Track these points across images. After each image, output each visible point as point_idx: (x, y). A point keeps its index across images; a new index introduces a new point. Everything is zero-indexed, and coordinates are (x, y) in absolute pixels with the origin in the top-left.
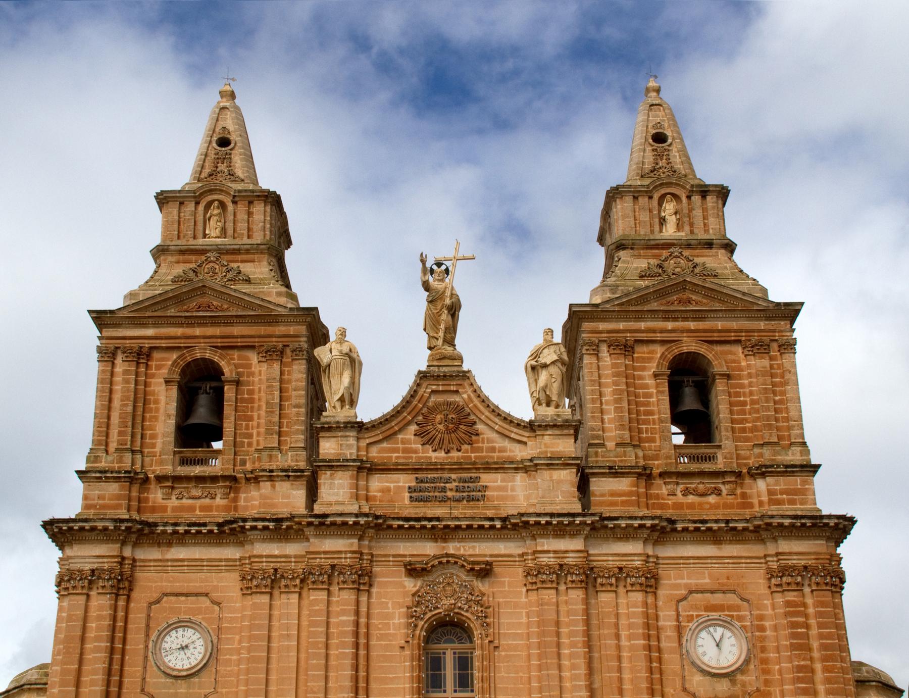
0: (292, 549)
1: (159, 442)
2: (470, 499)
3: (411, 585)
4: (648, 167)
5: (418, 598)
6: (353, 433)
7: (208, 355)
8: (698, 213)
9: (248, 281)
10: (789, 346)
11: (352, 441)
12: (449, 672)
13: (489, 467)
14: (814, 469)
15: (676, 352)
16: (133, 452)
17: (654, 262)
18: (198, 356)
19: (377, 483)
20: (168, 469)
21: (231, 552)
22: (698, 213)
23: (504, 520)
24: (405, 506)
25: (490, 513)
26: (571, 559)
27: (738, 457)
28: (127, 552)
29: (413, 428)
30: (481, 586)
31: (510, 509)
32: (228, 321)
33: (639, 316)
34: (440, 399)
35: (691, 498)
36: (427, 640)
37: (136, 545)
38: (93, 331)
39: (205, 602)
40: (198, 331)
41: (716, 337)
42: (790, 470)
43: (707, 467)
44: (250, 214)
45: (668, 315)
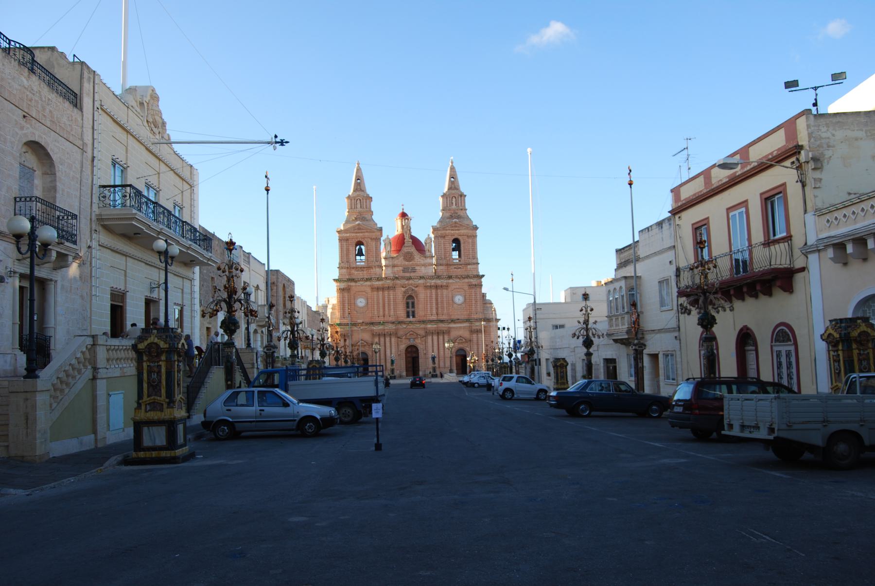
0: (380, 283)
1: (352, 259)
2: (414, 272)
3: (403, 289)
4: (450, 187)
5: (405, 292)
6: (391, 259)
7: (360, 240)
8: (460, 201)
9: (367, 220)
10: (476, 236)
11: (391, 261)
12: (410, 305)
13: (418, 265)
14: (479, 264)
15: (454, 238)
16: (347, 262)
17: (450, 214)
18: (358, 240)
19: (396, 269)
20: (354, 266)
21: (368, 283)
22: (460, 201)
23: (420, 277)
24: (402, 274)
25: (417, 275)
26: (432, 284)
27: (465, 261)
28: (349, 284)
29: (403, 257)
30: (416, 289)
31: (421, 275)
32: (364, 232)
33: (446, 230)
34: (407, 251)
35: (455, 269)
36: (406, 299)
37: (351, 282)
38: (337, 235)
39: (364, 293)
40: (358, 234)
41: (462, 234)
42: (474, 264)
43: (460, 263)
44: (366, 202)
45: (452, 230)
